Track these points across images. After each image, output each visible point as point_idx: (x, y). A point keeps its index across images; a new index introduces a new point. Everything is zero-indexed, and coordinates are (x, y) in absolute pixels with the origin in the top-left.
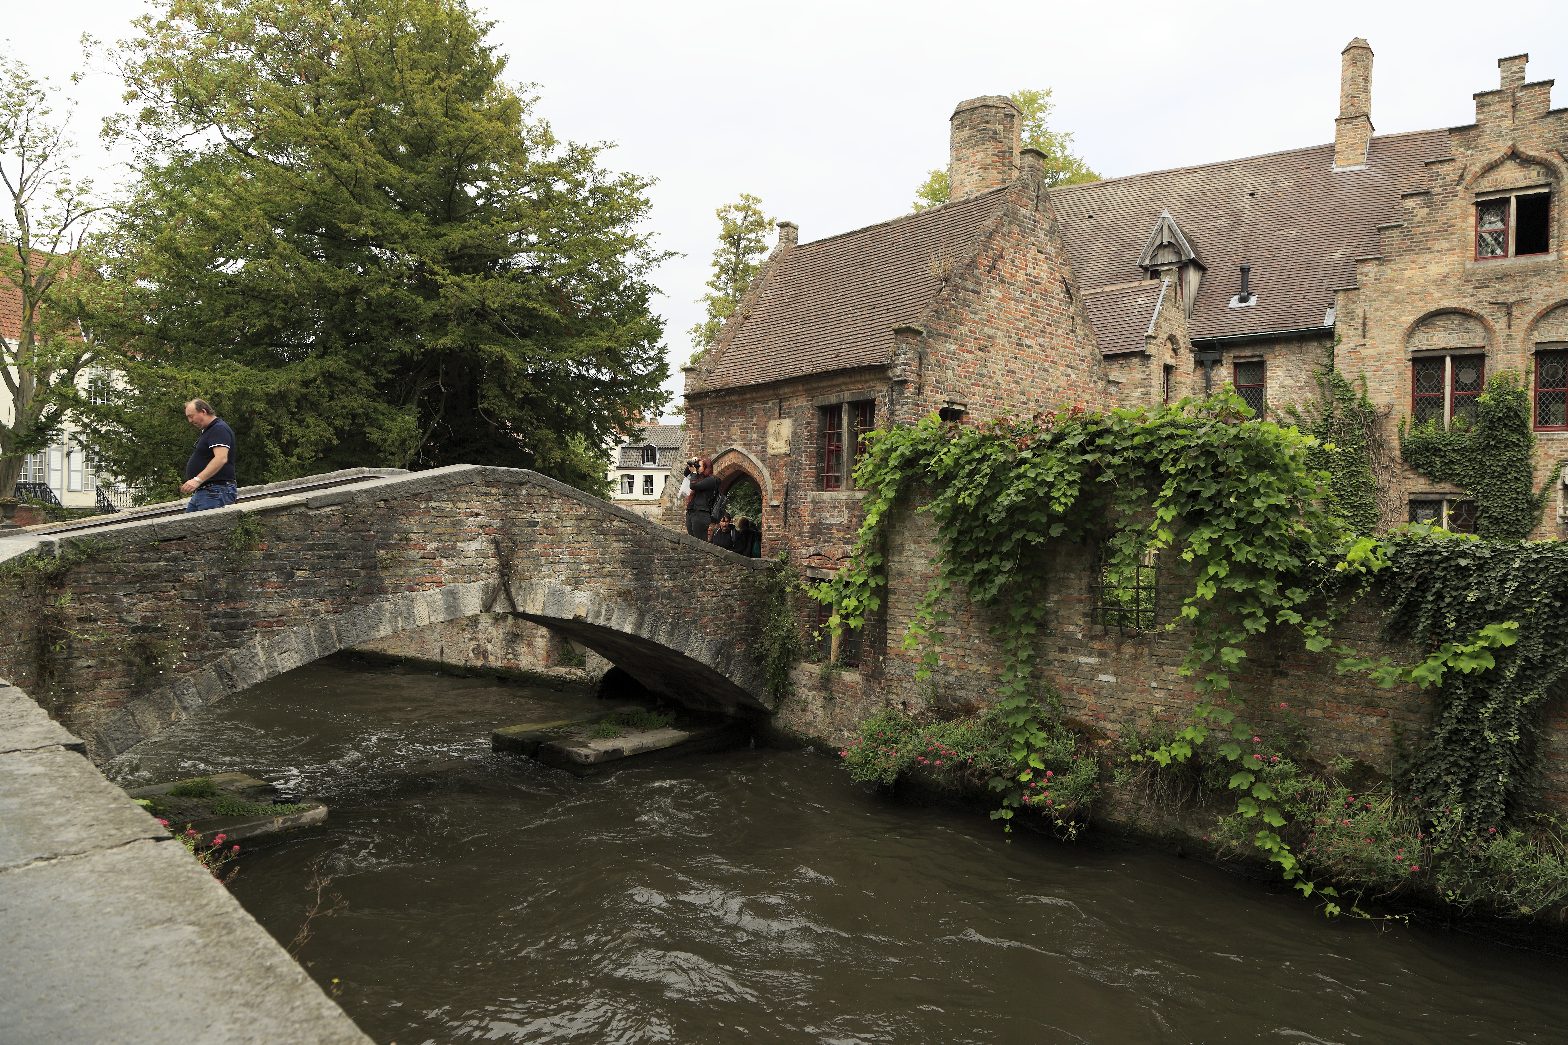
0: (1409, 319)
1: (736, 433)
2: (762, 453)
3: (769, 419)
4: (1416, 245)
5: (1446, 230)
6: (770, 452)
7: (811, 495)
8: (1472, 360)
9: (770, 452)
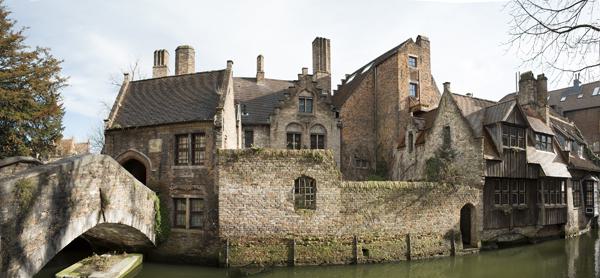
0: (286, 124)
1: (132, 144)
2: (147, 152)
3: (150, 139)
4: (287, 106)
5: (293, 104)
6: (150, 151)
7: (173, 167)
8: (298, 135)
9: (150, 151)
